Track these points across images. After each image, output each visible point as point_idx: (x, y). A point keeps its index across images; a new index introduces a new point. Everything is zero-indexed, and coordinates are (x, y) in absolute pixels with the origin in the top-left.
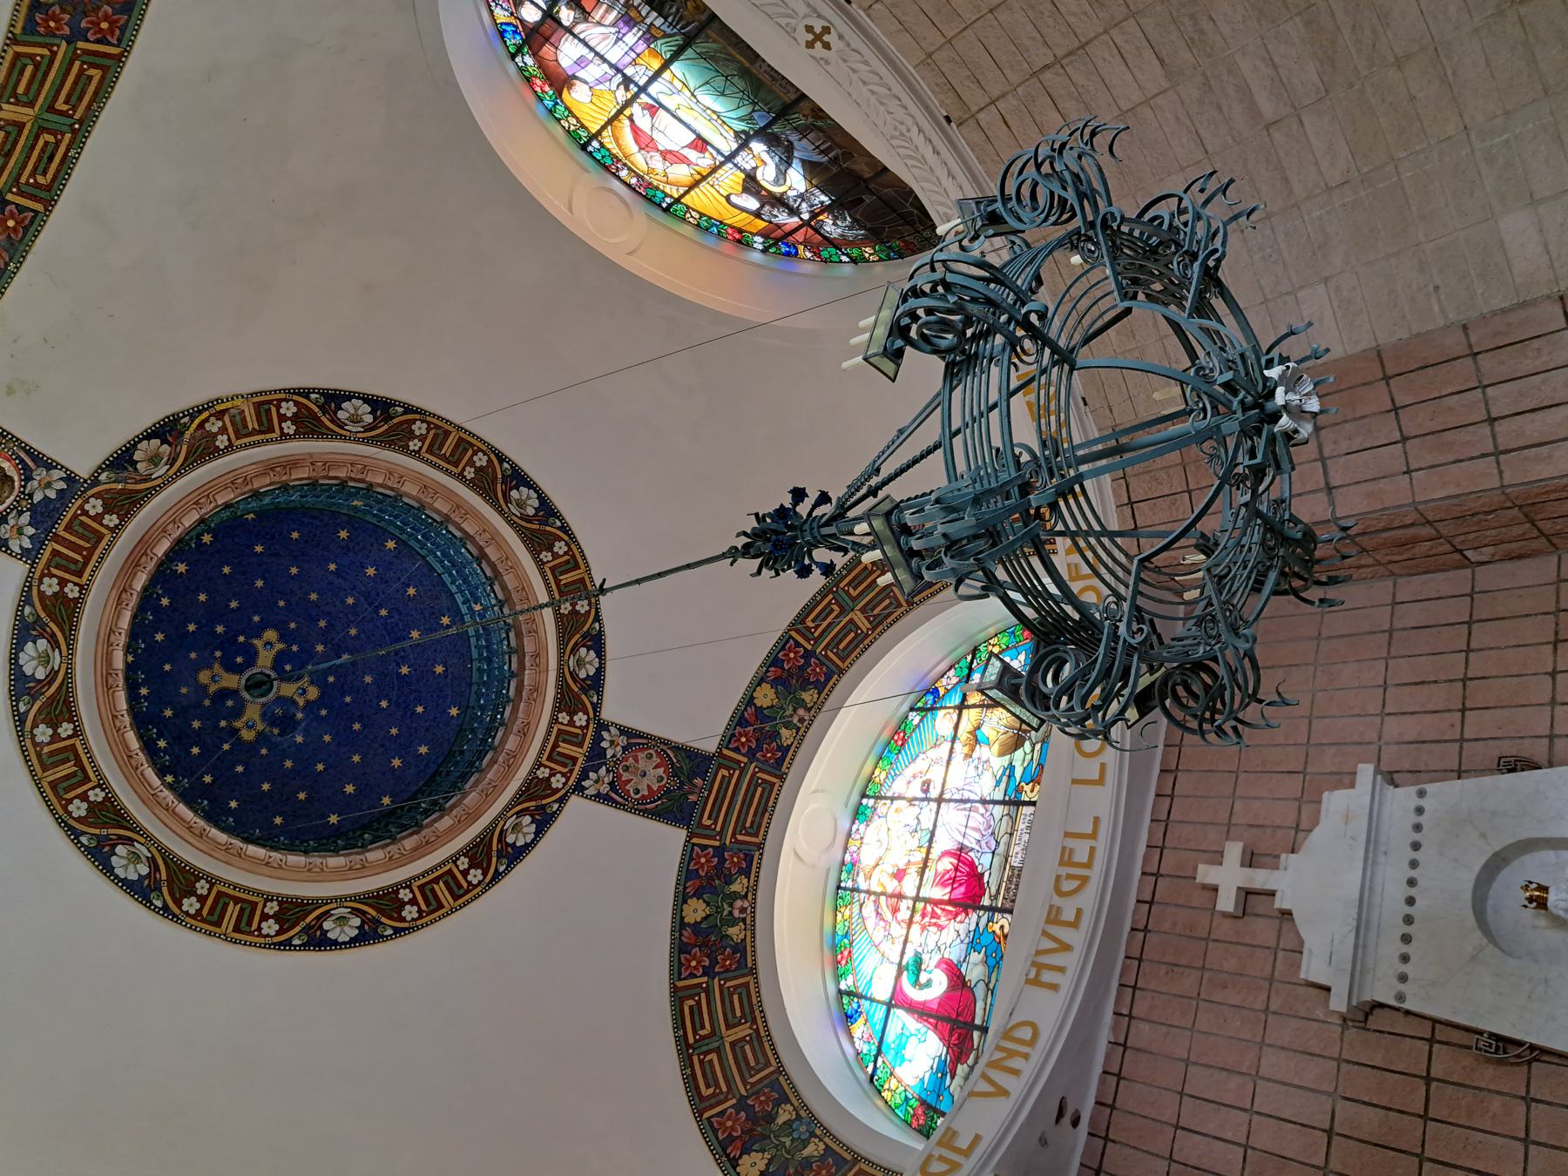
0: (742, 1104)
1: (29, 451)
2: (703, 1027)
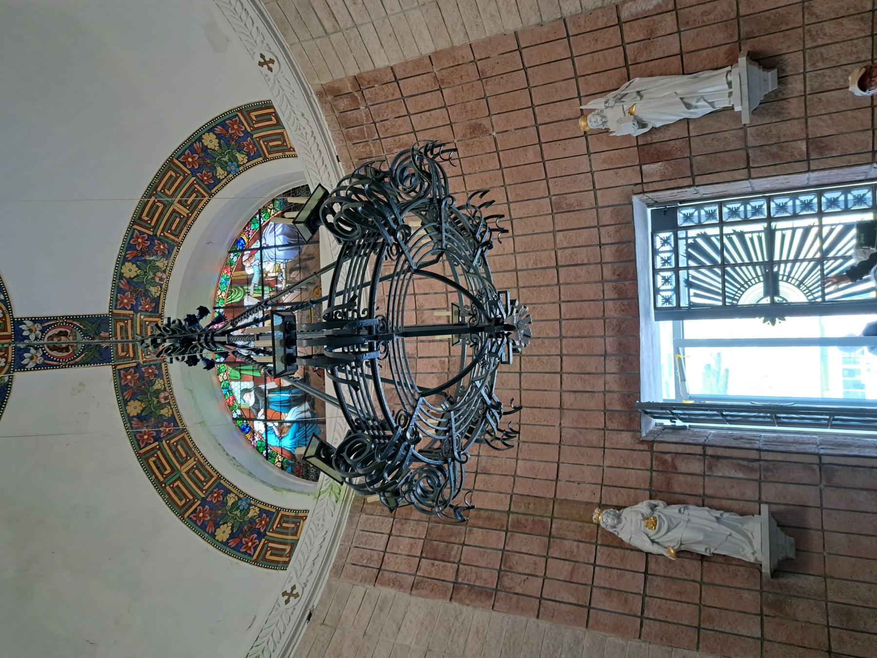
1: (53, 367)
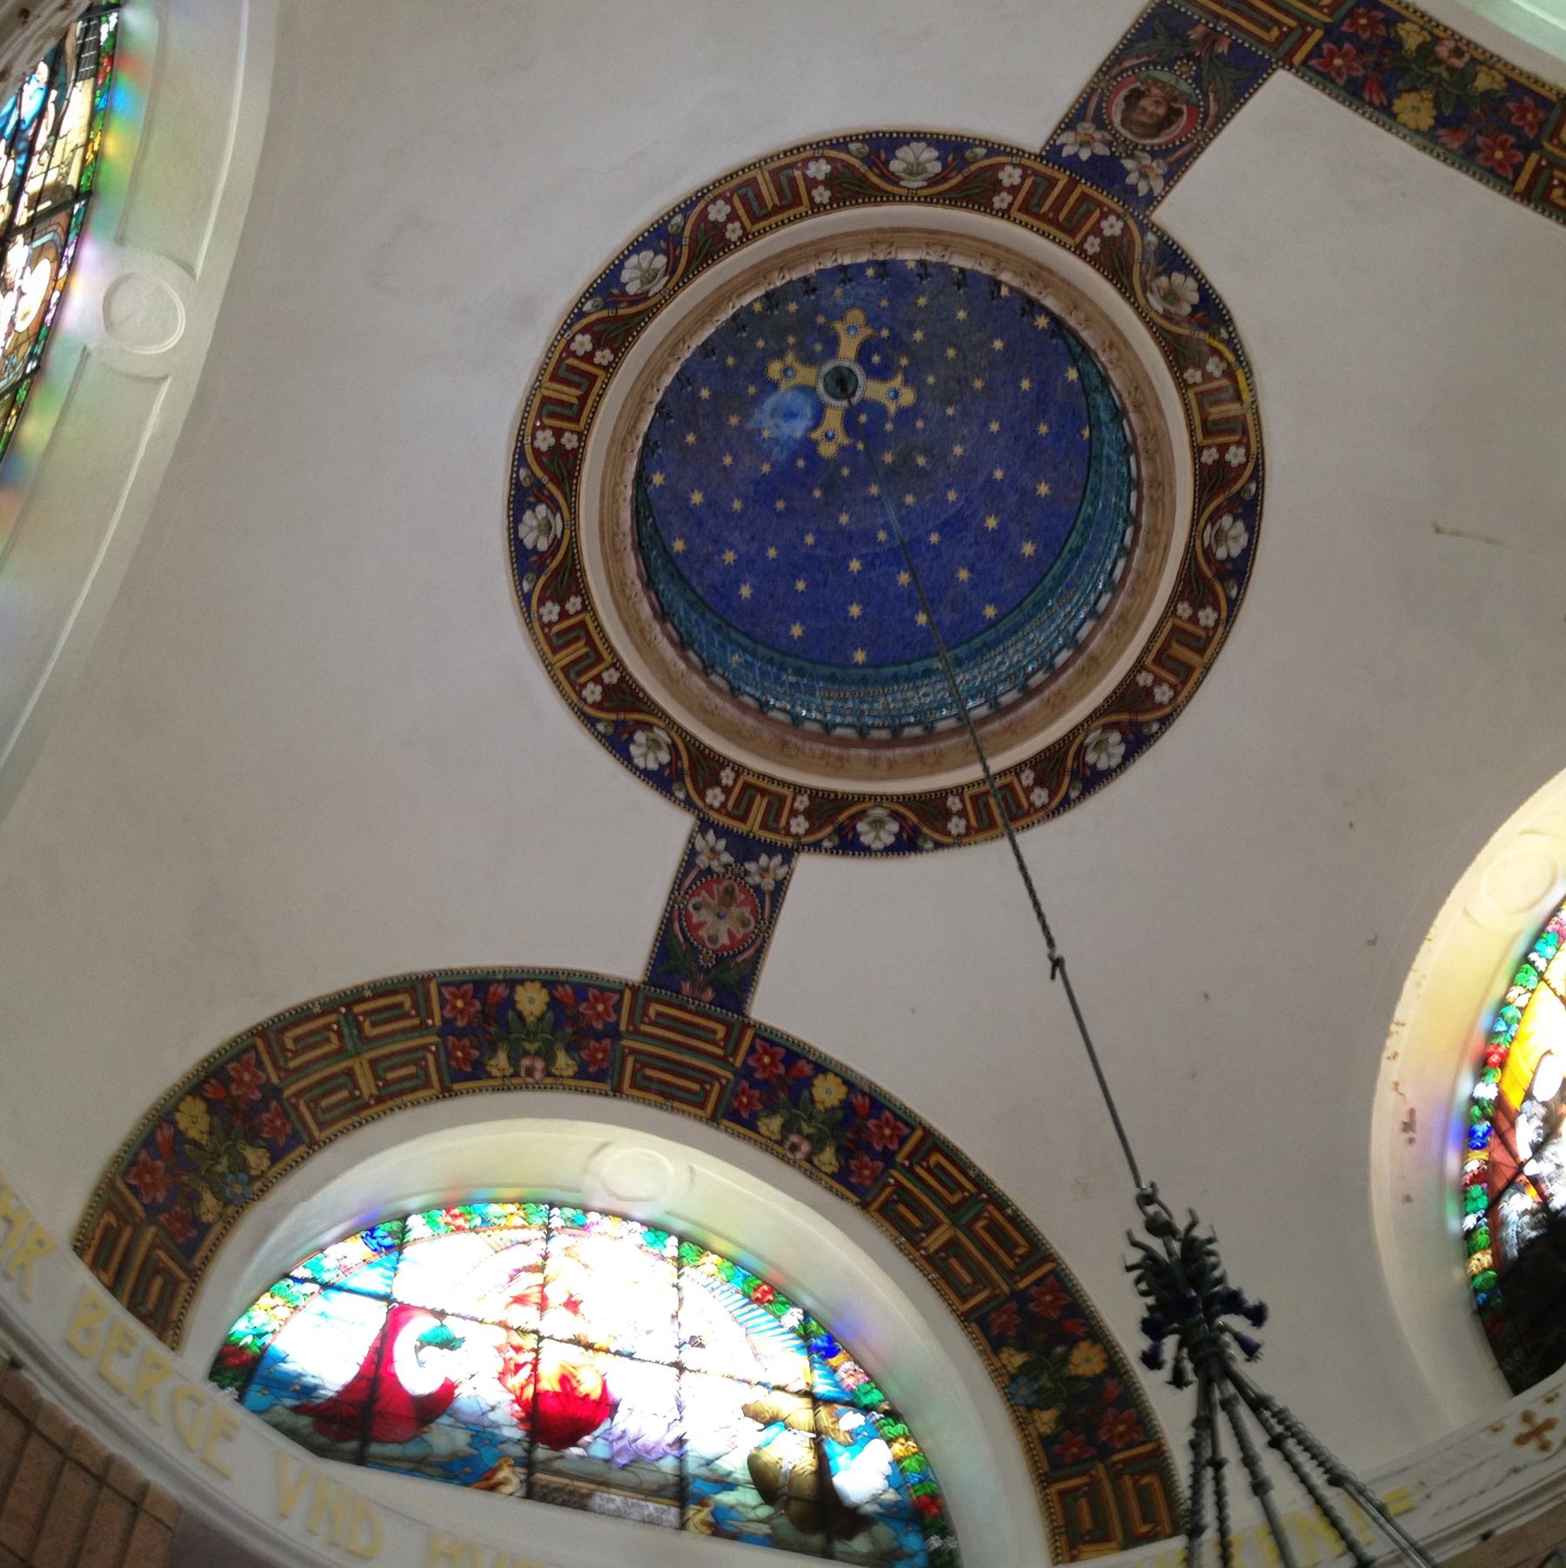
0: (274, 1092)
2: (374, 1025)
